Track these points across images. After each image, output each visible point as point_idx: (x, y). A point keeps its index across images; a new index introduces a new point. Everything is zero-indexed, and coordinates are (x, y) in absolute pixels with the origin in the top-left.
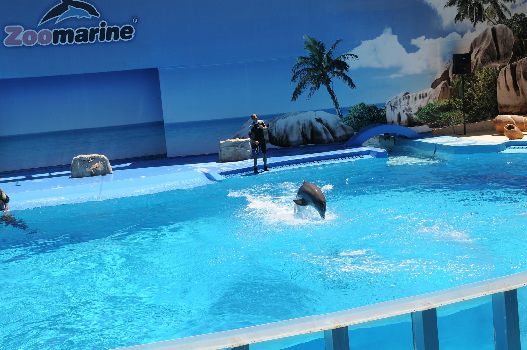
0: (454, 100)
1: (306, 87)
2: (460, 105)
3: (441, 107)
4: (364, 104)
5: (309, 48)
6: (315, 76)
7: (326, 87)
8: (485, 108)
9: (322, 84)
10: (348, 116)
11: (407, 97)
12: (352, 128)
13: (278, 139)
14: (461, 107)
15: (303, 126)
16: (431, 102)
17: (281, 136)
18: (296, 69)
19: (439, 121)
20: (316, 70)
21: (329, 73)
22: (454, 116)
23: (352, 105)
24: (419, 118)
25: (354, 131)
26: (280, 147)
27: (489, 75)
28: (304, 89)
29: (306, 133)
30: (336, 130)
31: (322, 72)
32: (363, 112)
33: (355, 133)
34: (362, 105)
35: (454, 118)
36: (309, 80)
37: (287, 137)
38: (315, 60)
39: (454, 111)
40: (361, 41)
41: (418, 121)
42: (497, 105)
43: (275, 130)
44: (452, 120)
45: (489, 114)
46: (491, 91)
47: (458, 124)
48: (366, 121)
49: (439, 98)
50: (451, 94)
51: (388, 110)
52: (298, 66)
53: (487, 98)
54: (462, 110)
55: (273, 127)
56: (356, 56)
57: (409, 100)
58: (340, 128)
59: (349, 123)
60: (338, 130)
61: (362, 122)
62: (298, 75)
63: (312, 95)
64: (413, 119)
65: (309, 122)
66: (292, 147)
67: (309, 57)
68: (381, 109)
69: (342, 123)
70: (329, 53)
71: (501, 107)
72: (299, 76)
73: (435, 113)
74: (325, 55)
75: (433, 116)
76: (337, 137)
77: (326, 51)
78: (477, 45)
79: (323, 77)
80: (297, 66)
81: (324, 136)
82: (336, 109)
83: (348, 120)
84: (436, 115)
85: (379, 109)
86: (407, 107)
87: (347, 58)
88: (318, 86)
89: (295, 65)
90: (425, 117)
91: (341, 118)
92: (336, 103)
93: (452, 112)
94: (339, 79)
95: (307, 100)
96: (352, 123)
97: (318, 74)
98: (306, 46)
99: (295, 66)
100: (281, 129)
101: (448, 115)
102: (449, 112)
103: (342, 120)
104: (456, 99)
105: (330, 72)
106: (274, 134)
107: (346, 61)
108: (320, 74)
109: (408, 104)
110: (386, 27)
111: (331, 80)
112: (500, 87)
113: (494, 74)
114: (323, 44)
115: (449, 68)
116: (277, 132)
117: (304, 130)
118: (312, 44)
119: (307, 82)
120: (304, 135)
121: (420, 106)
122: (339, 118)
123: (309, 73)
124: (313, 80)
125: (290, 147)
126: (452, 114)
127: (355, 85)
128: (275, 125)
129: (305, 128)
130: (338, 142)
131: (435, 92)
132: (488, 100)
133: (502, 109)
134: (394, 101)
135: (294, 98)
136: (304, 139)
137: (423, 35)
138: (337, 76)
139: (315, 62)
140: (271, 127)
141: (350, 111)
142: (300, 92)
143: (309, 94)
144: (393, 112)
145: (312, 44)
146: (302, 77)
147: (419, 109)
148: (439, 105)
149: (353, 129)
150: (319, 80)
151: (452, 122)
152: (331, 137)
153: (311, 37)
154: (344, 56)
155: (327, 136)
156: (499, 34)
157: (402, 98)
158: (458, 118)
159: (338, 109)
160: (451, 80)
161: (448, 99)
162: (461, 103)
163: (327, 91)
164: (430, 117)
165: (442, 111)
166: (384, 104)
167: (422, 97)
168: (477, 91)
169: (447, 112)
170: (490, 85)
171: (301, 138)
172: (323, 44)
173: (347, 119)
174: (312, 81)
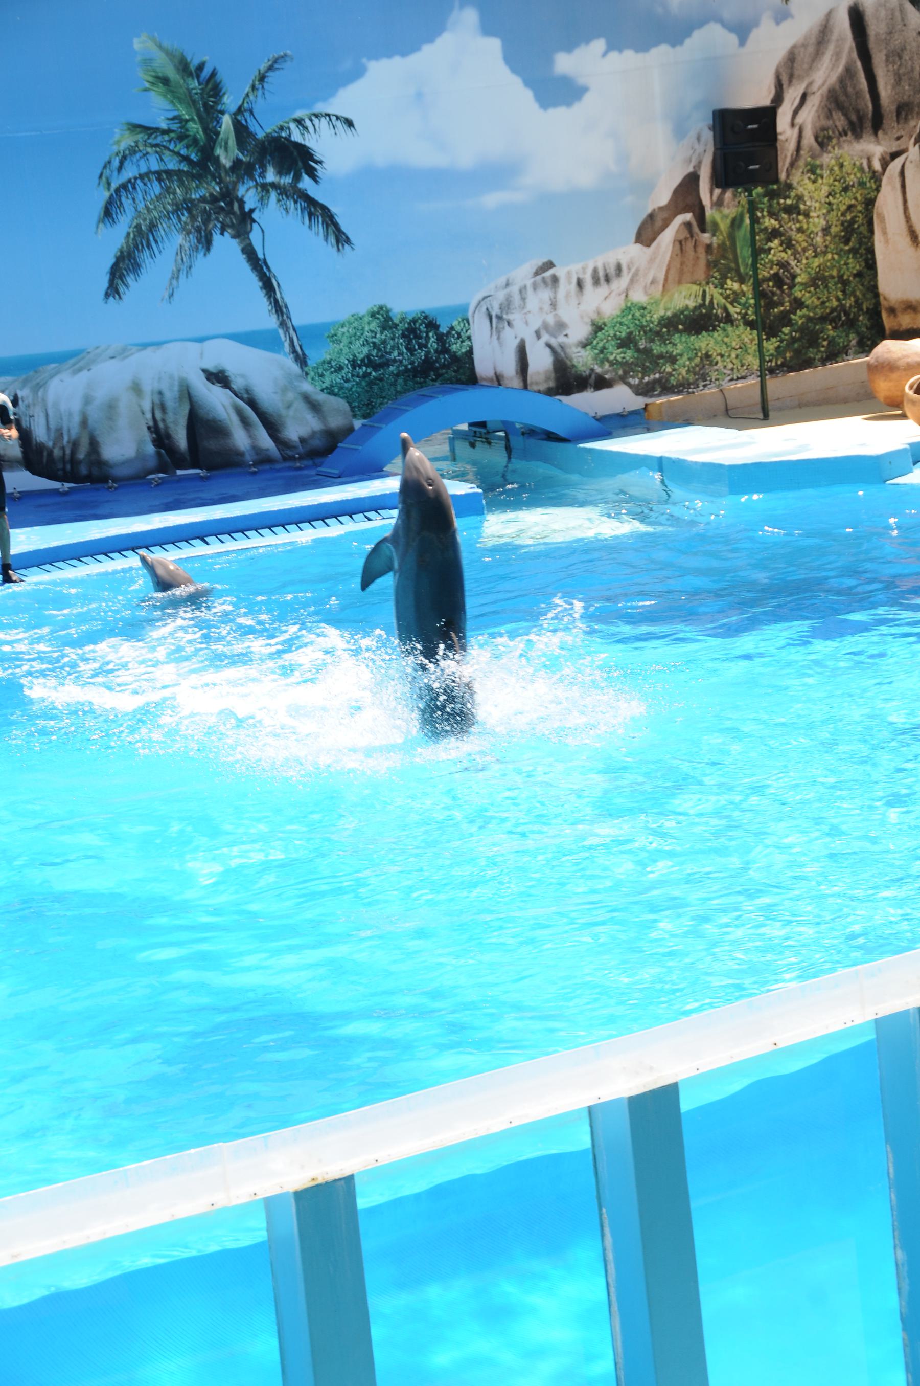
0: (722, 288)
1: (158, 247)
2: (745, 306)
3: (675, 315)
4: (388, 311)
5: (161, 88)
6: (192, 201)
7: (241, 243)
8: (835, 314)
9: (222, 234)
10: (328, 357)
11: (549, 281)
12: (347, 404)
13: (57, 452)
14: (746, 314)
15: (157, 401)
16: (639, 296)
17: (68, 442)
18: (115, 173)
19: (669, 369)
20: (193, 177)
21: (248, 190)
22: (724, 350)
23: (343, 315)
24: (595, 359)
25: (355, 416)
26: (68, 485)
27: (846, 189)
28: (153, 255)
29: (167, 427)
30: (283, 412)
31: (218, 183)
32: (384, 342)
33: (358, 424)
34: (378, 313)
35: (722, 356)
36: (169, 218)
37: (94, 445)
38: (187, 136)
39: (724, 330)
40: (364, 60)
41: (592, 370)
42: (878, 304)
43: (42, 415)
44: (717, 363)
45: (852, 336)
46: (854, 251)
47: (738, 379)
48: (397, 375)
49: (666, 280)
50: (711, 265)
51: (480, 332)
52: (122, 163)
53: (841, 277)
54: (751, 325)
55: (34, 405)
56: (349, 123)
57: (555, 293)
58: (300, 405)
59: (332, 386)
60: (291, 412)
61: (381, 380)
62: (123, 199)
63: (182, 276)
64: (574, 366)
65: (176, 383)
66: (115, 485)
67: (164, 126)
68: (452, 328)
69: (307, 387)
70: (240, 110)
71: (892, 311)
72: (127, 202)
73: (652, 341)
74: (226, 120)
75: (647, 352)
76: (290, 440)
77: (230, 102)
78: (796, 73)
79: (222, 204)
80: (116, 163)
81: (240, 439)
82: (281, 332)
83: (327, 374)
84: (657, 349)
85: (444, 329)
86: (551, 320)
87: (311, 129)
88: (207, 243)
89: (110, 158)
90: (616, 354)
91: (301, 368)
92: (279, 308)
93: (716, 334)
94: (287, 212)
95: (167, 297)
96: (346, 385)
97: (203, 192)
98: (151, 79)
99: (109, 162)
100: (70, 414)
101: (703, 345)
102: (704, 333)
103: (307, 374)
104: (729, 282)
105: (252, 183)
106: (40, 434)
107: (310, 141)
108: (211, 195)
109: (554, 305)
110: (457, 4)
111: (255, 216)
112: (884, 233)
113: (862, 184)
114: (213, 74)
115: (700, 163)
116: (53, 426)
117: (159, 415)
118: (171, 73)
119: (163, 226)
120: (161, 438)
121: (599, 313)
122: (295, 368)
123: (168, 190)
124: (184, 219)
125: (107, 482)
126: (716, 342)
127: (350, 236)
128: (44, 400)
129: (163, 408)
130: (292, 458)
131: (652, 260)
132: (845, 283)
133: (895, 316)
134: (501, 296)
135: (113, 291)
136: (163, 451)
137: (598, 36)
138: (279, 201)
139: (187, 147)
140: (28, 406)
141: (335, 339)
142: (136, 267)
143: (173, 274)
144: (498, 338)
145: (171, 73)
146: (141, 207)
147: (593, 324)
148: (666, 309)
149: (347, 408)
150: (209, 216)
151: (717, 370)
152: (266, 442)
153: (166, 44)
154: (299, 122)
155: (251, 436)
156: (875, 28)
157: (529, 283)
158: (737, 357)
159: (287, 330)
160: (709, 212)
161: (700, 284)
162: (748, 299)
163: (242, 258)
164: (636, 355)
165: (678, 331)
166: (465, 309)
167: (603, 278)
168: (805, 250)
169: (698, 333)
170: (849, 229)
171: (150, 449)
172: (213, 74)
173: (326, 370)
174: (180, 220)
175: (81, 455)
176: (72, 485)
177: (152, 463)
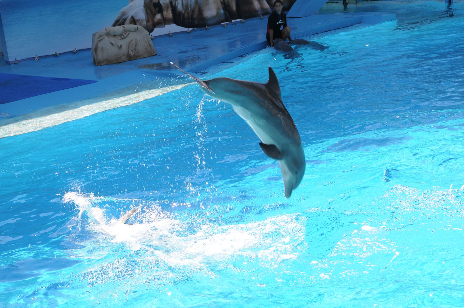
13: (186, 15)
17: (190, 11)
26: (190, 29)
37: (201, 12)
106: (180, 7)
116: (184, 4)
125: (205, 27)
136: (227, 12)
171: (222, 11)
175: (195, 16)
176: (192, 29)
177: (223, 18)
